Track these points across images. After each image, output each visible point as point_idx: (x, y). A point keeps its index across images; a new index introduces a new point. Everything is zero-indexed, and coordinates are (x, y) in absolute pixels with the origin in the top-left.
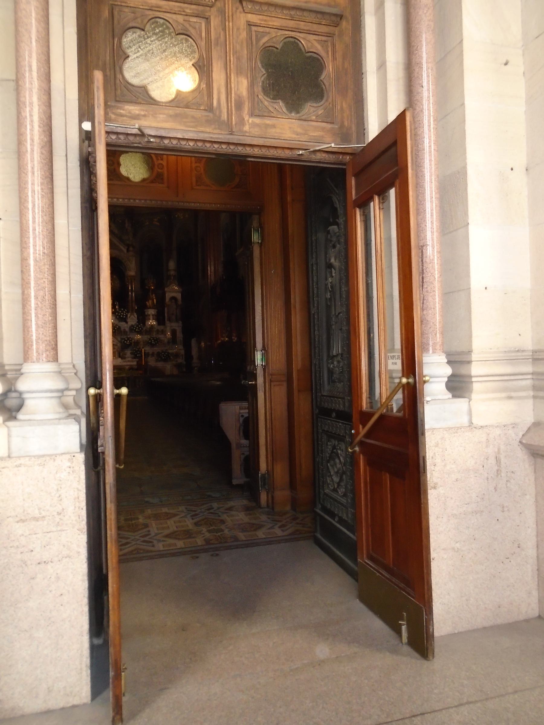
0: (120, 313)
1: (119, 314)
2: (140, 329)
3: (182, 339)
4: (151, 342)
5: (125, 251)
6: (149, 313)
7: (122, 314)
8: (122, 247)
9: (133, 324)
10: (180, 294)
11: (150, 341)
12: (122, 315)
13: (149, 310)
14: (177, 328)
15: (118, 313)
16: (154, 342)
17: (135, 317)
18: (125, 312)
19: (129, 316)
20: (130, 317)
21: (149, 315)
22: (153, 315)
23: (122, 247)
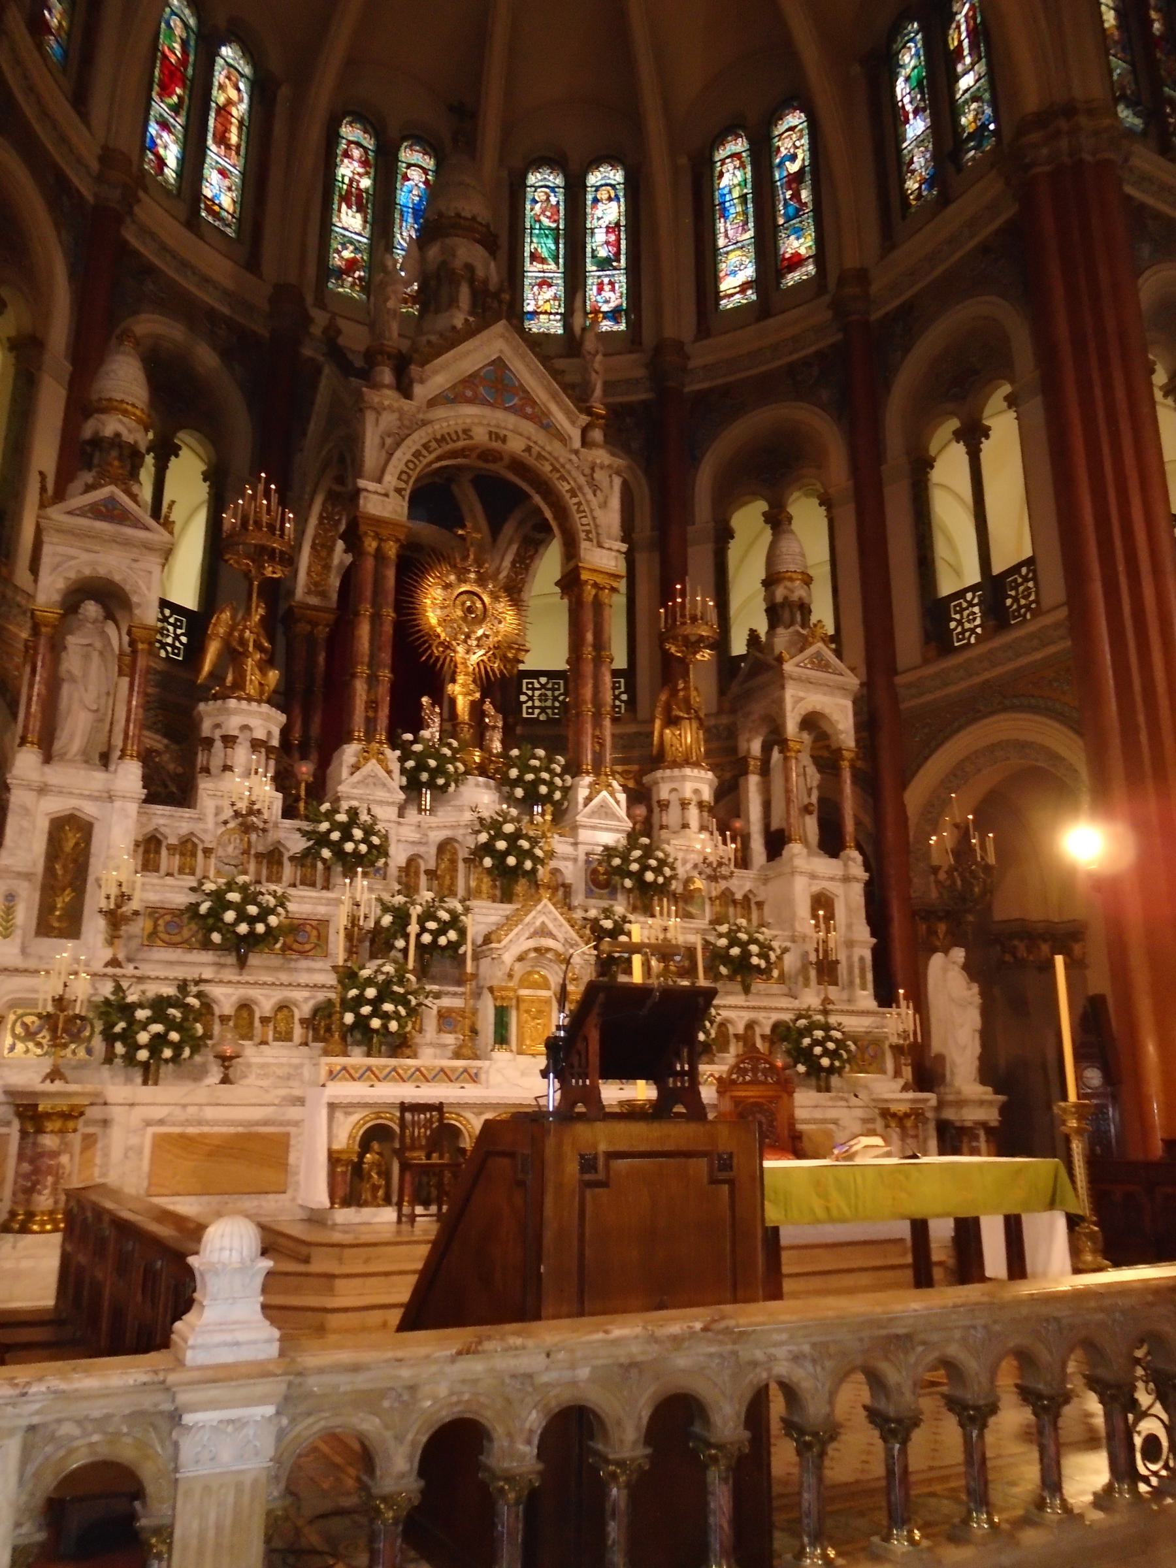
0: (535, 770)
1: (530, 777)
2: (667, 871)
3: (868, 955)
4: (746, 955)
5: (575, 434)
6: (688, 791)
7: (545, 776)
8: (560, 417)
9: (609, 838)
10: (848, 704)
11: (735, 951)
12: (544, 782)
13: (688, 771)
14: (836, 888)
15: (525, 768)
16: (759, 956)
17: (618, 802)
18: (558, 769)
19: (583, 793)
20: (588, 800)
21: (684, 804)
22: (701, 805)
23: (560, 417)
